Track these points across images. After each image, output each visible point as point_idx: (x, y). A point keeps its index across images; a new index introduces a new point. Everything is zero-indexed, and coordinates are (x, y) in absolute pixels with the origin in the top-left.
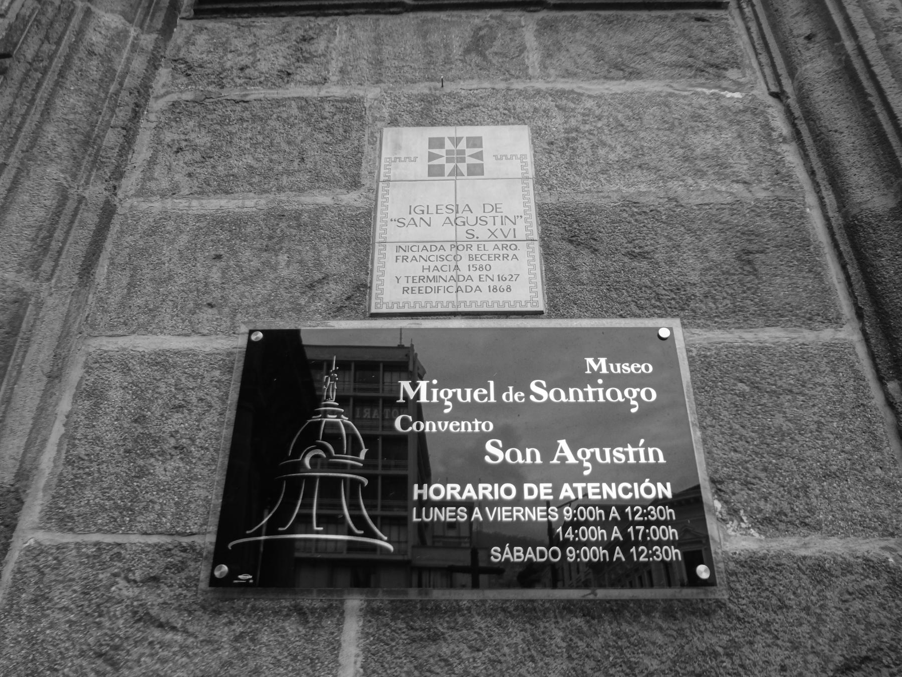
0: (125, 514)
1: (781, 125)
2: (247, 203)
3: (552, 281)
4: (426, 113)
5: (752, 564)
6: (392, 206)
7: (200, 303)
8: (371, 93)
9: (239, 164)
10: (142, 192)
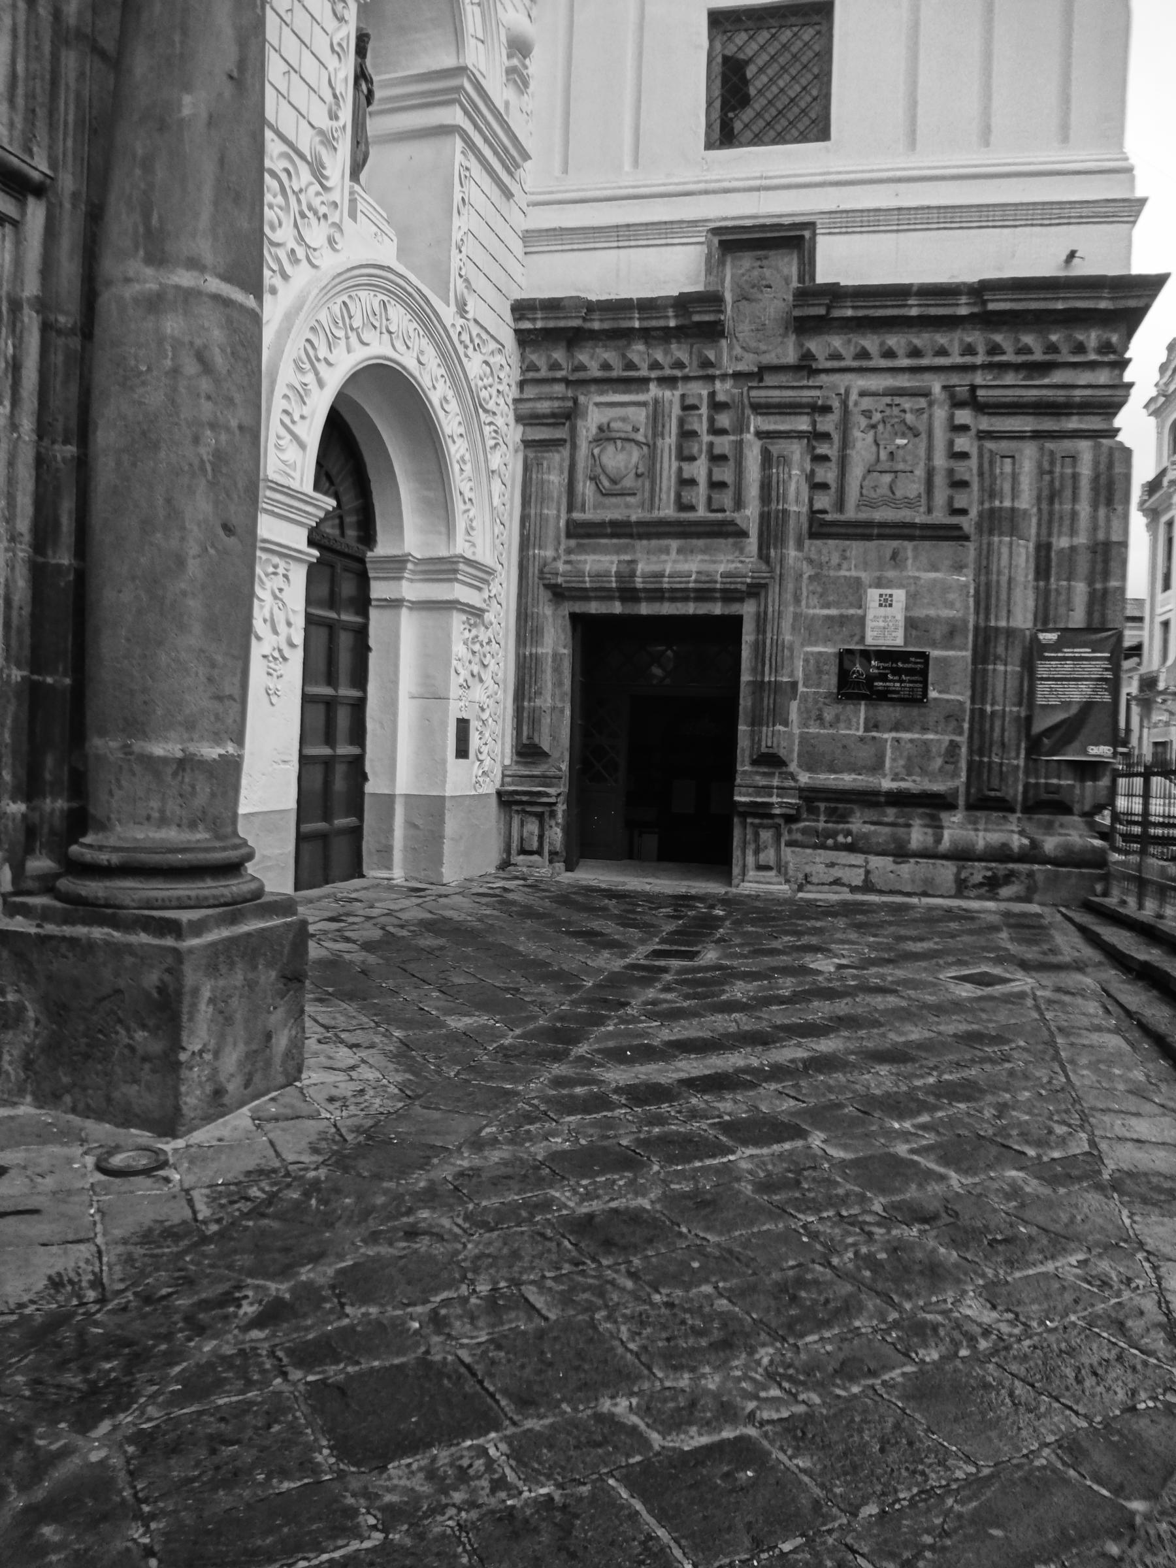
0: (819, 685)
1: (972, 591)
2: (833, 612)
3: (906, 637)
4: (879, 584)
5: (935, 699)
6: (870, 615)
7: (827, 640)
8: (863, 575)
9: (831, 598)
10: (808, 607)
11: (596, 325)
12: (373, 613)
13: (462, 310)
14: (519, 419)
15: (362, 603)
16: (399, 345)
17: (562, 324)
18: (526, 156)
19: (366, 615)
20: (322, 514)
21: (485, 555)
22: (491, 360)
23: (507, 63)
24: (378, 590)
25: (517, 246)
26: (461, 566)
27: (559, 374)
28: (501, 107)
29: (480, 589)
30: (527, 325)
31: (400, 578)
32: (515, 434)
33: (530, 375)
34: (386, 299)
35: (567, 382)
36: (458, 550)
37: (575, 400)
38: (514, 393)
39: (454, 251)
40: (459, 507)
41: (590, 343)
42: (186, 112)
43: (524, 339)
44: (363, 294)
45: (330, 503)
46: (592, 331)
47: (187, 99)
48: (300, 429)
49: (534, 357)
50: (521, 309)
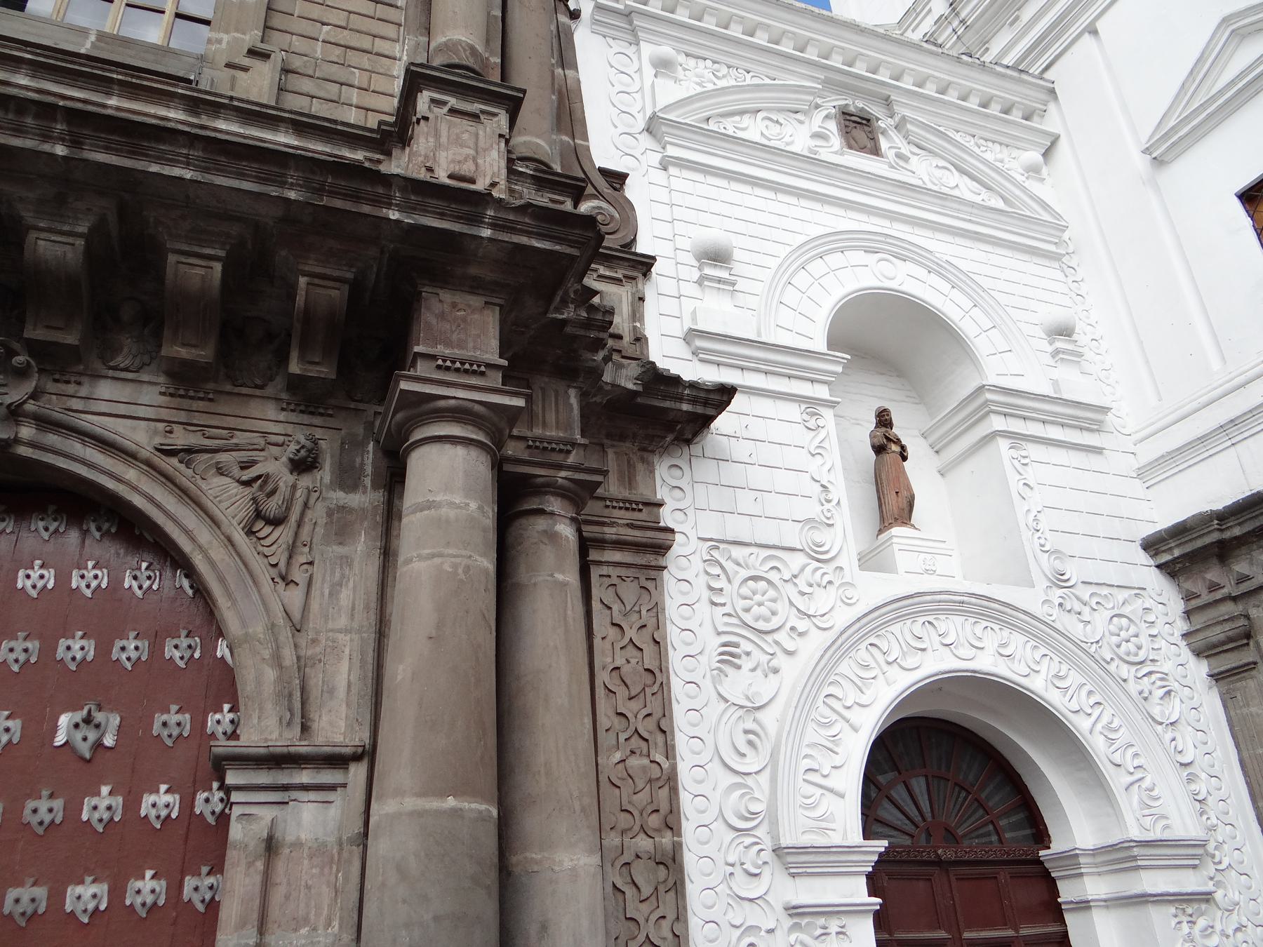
11: (1237, 531)
12: (1069, 918)
13: (1059, 580)
14: (1198, 654)
15: (1055, 911)
16: (966, 652)
17: (1199, 543)
18: (1104, 410)
19: (1063, 922)
20: (875, 858)
21: (1184, 825)
22: (1126, 610)
23: (1050, 349)
24: (1067, 892)
25: (1137, 487)
26: (1136, 851)
27: (1219, 595)
28: (1047, 390)
29: (1194, 867)
30: (1166, 558)
31: (1081, 875)
32: (1200, 669)
33: (1195, 603)
34: (931, 618)
35: (1234, 599)
36: (1135, 833)
37: (1247, 617)
38: (1182, 626)
39: (1026, 534)
40: (1117, 780)
41: (1244, 550)
42: (399, 677)
43: (1171, 570)
44: (896, 628)
45: (881, 845)
46: (1236, 538)
47: (401, 667)
48: (835, 782)
49: (1188, 585)
50: (1152, 545)
